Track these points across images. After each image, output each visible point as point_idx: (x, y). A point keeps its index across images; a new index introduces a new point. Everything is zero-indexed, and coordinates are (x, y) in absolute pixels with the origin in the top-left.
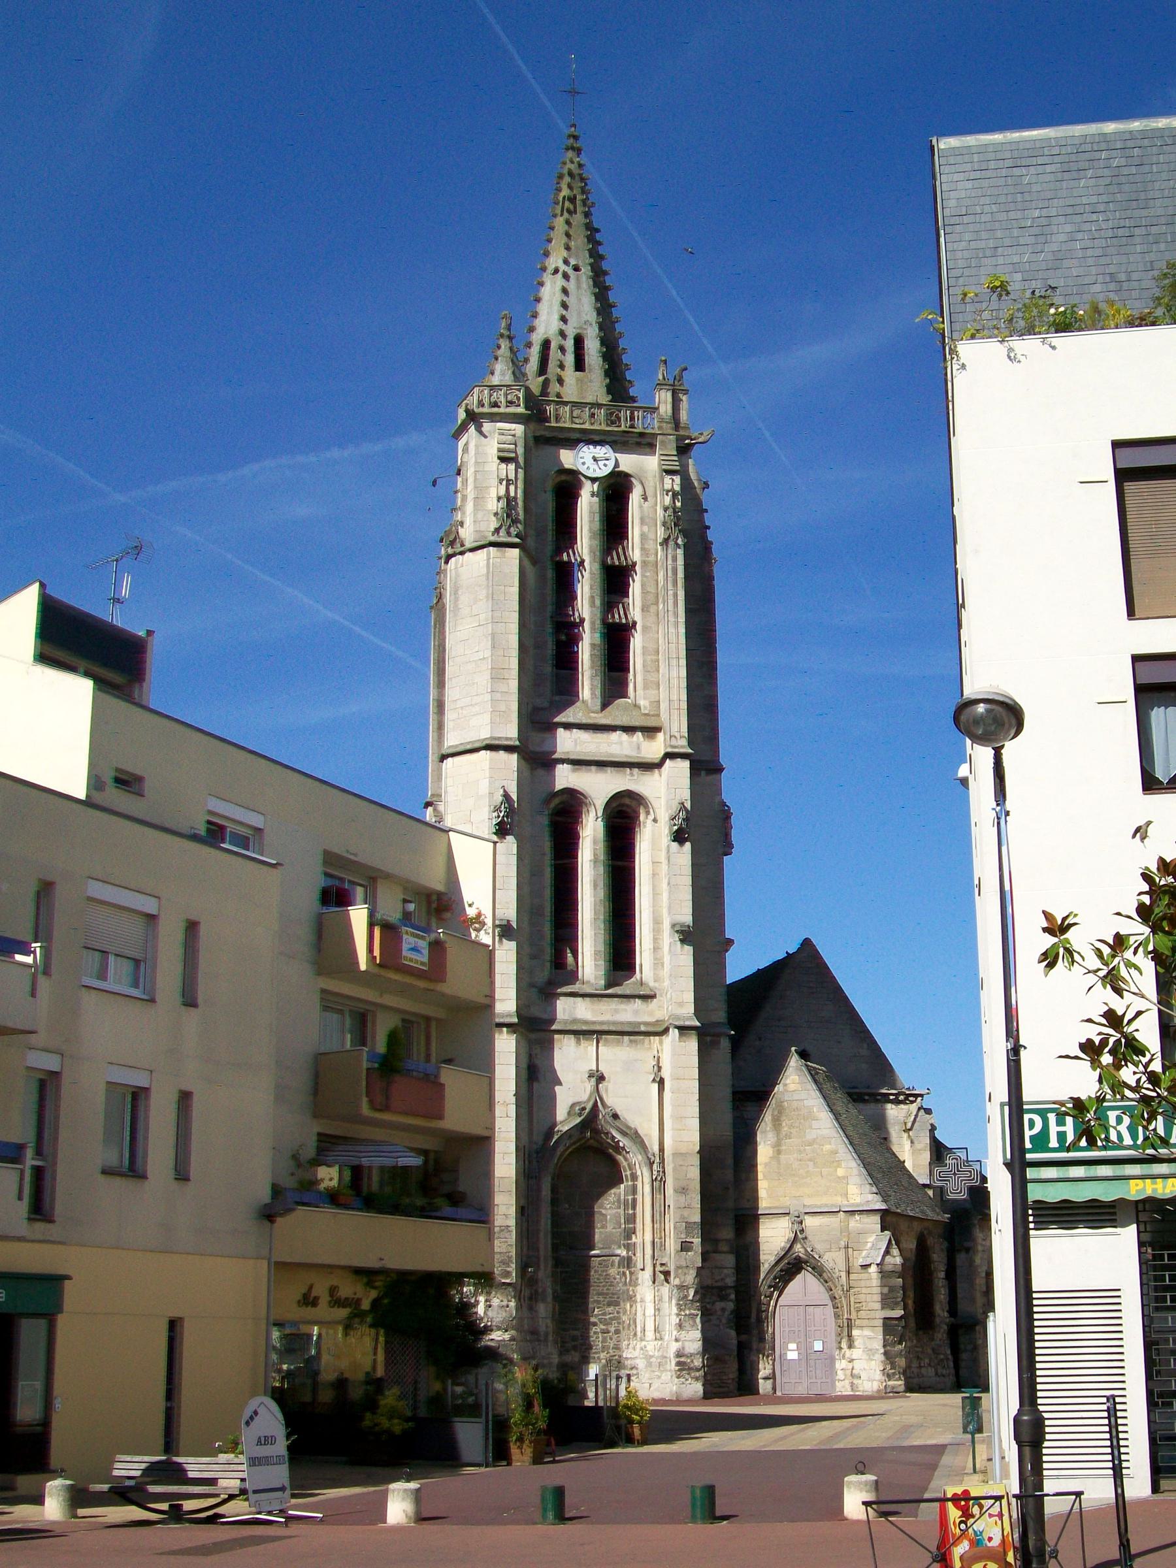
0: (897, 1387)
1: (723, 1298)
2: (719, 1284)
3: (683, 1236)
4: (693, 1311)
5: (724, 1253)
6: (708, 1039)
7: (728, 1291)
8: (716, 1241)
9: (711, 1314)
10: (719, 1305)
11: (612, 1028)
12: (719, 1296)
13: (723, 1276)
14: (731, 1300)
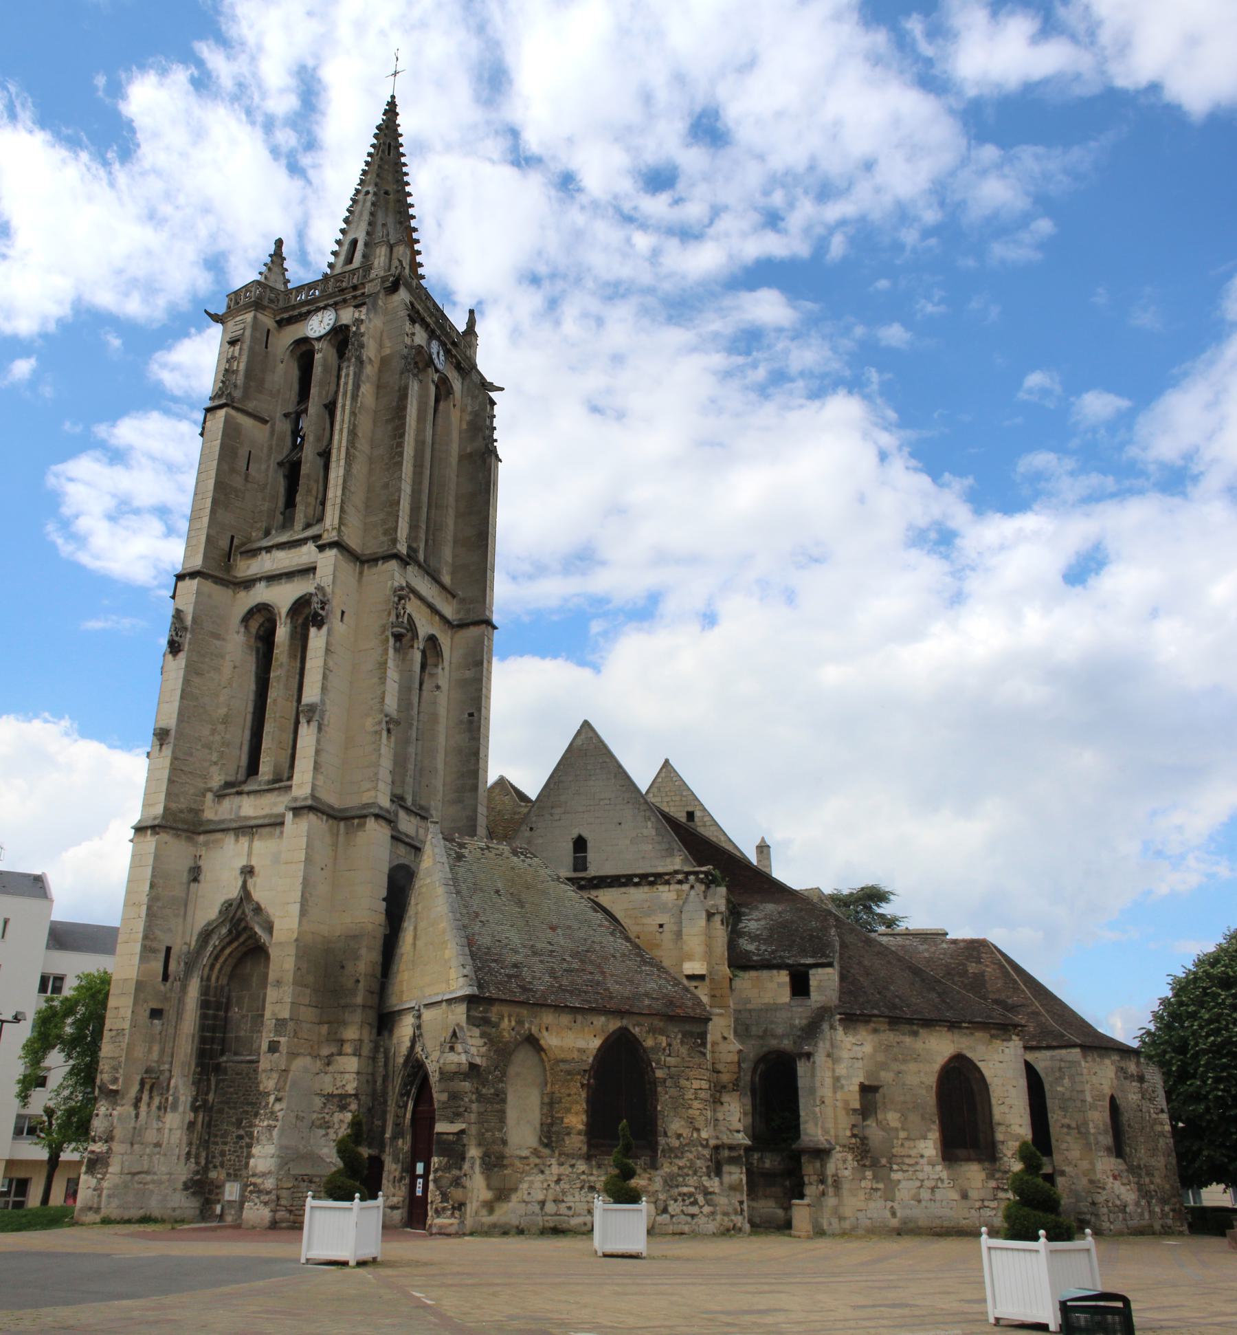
0: (446, 1227)
1: (343, 1108)
2: (339, 1092)
3: (272, 1035)
4: (271, 1122)
5: (347, 1055)
6: (356, 821)
7: (348, 1100)
8: (342, 1042)
9: (329, 1127)
10: (338, 1116)
11: (266, 821)
12: (339, 1106)
13: (344, 1083)
14: (350, 1111)
